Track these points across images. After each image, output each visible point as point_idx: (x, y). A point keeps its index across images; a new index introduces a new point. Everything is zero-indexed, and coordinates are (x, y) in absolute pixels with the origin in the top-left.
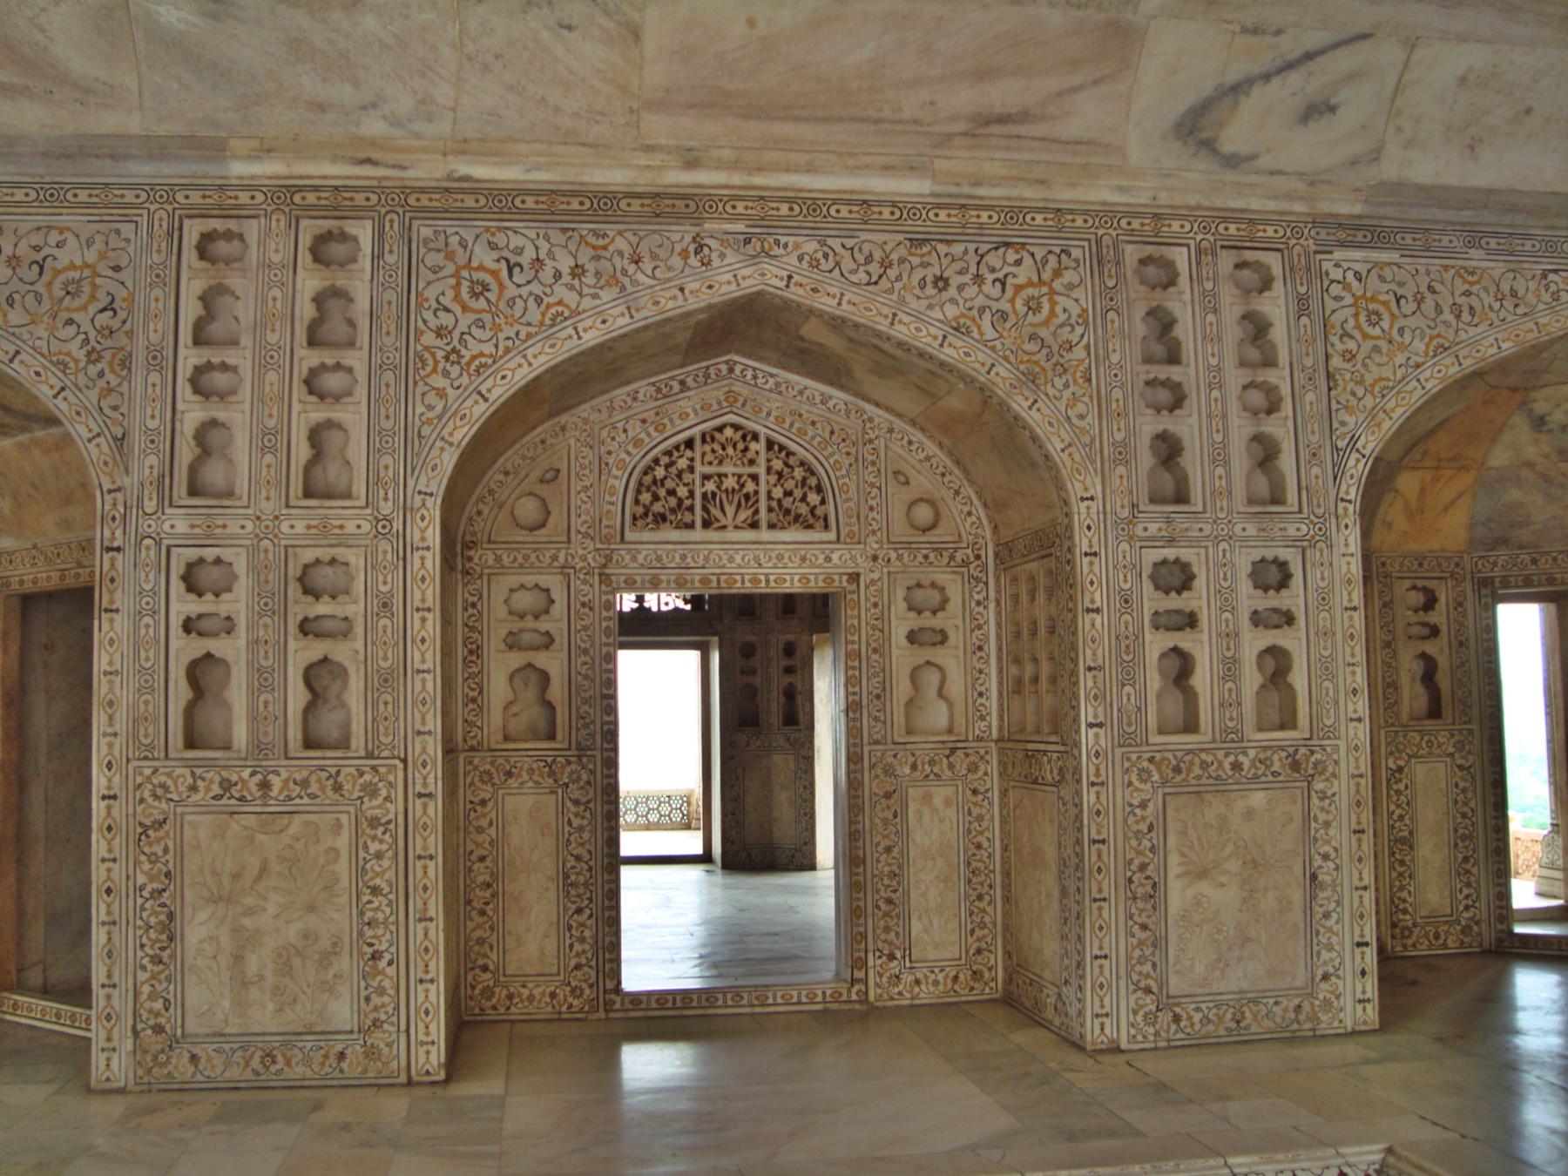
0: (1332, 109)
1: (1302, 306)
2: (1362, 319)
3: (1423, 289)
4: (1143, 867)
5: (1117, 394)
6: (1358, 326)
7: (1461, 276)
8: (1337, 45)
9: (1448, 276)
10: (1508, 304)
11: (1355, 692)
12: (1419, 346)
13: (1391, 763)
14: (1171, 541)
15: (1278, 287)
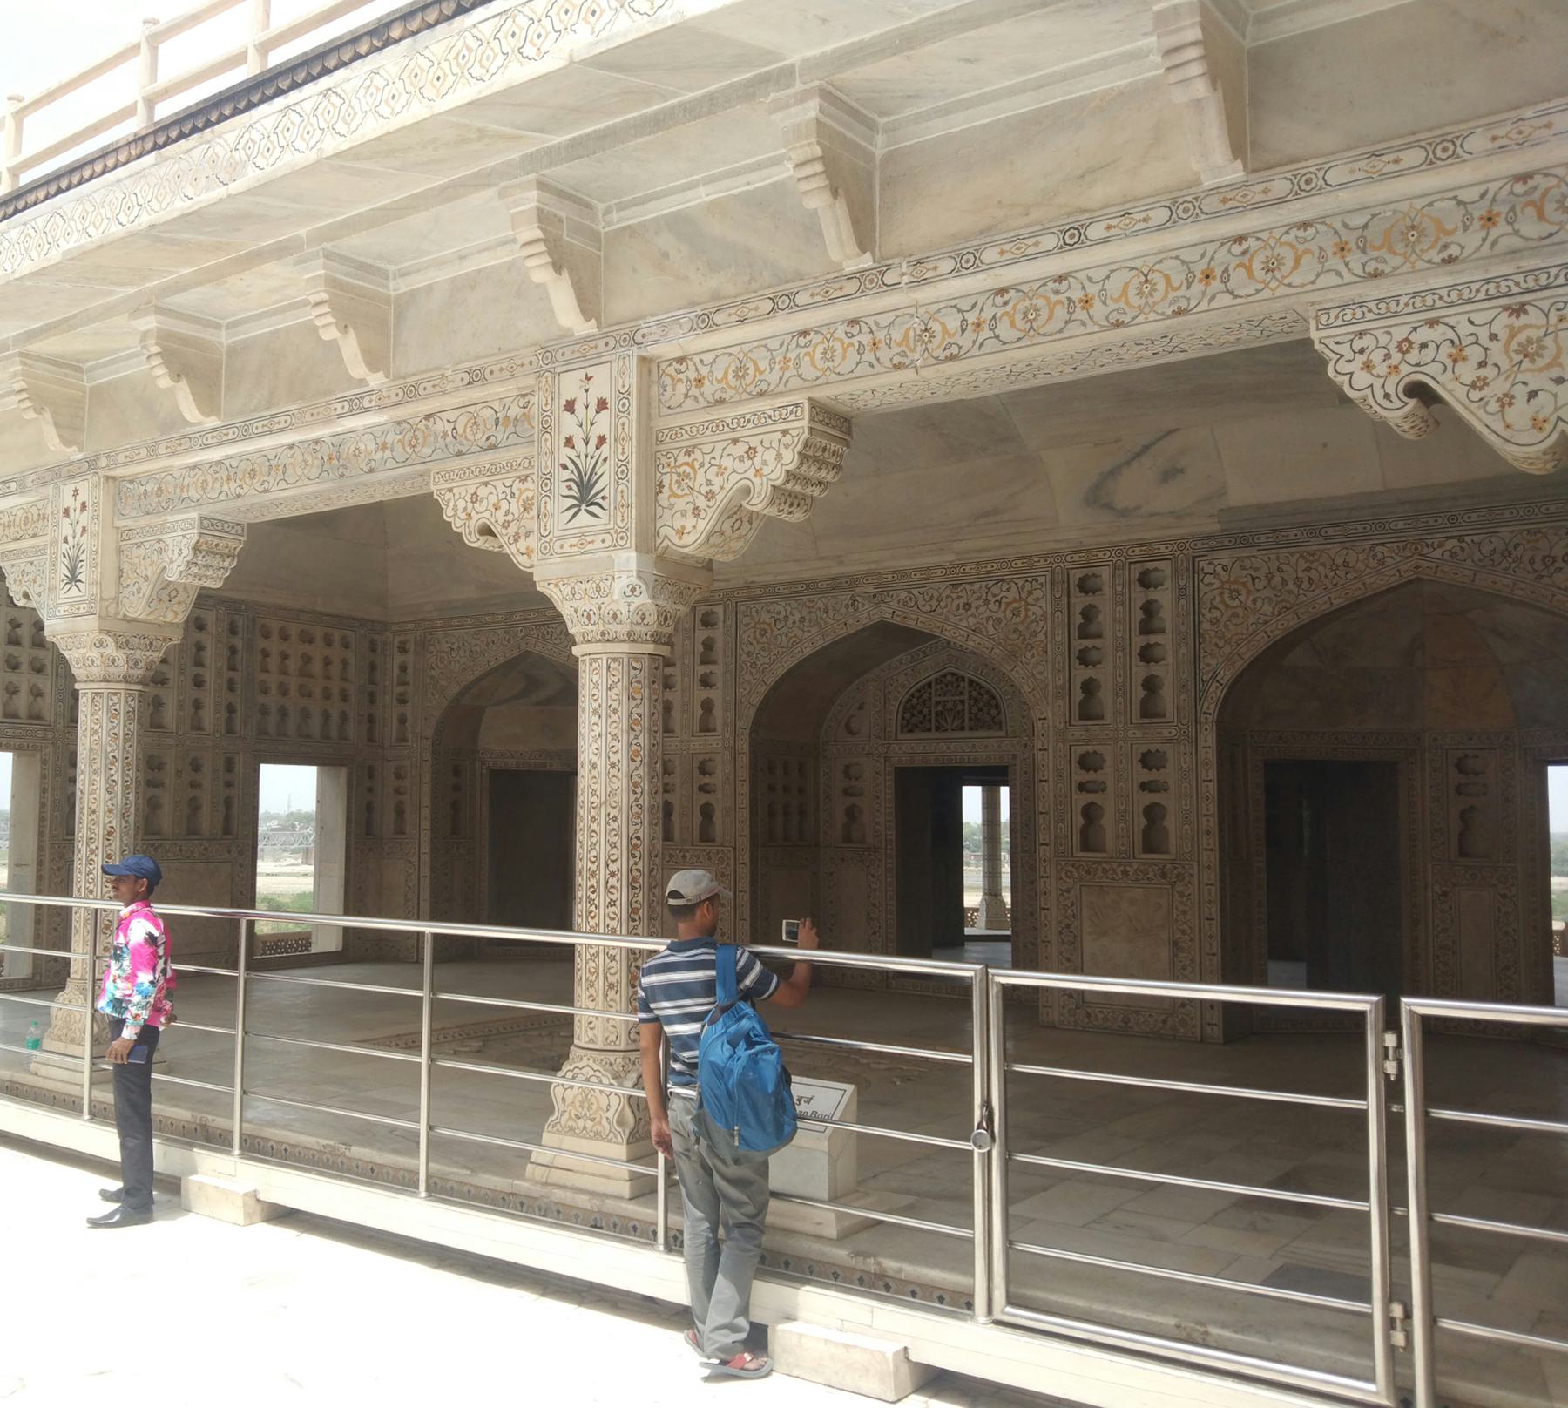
0: (1182, 471)
1: (1181, 593)
2: (1226, 596)
3: (1274, 570)
4: (1068, 926)
5: (1059, 659)
6: (1223, 601)
7: (1302, 556)
8: (1160, 439)
9: (1293, 560)
10: (1341, 573)
11: (1209, 833)
12: (1267, 609)
13: (1437, 889)
14: (1088, 742)
15: (1168, 583)
